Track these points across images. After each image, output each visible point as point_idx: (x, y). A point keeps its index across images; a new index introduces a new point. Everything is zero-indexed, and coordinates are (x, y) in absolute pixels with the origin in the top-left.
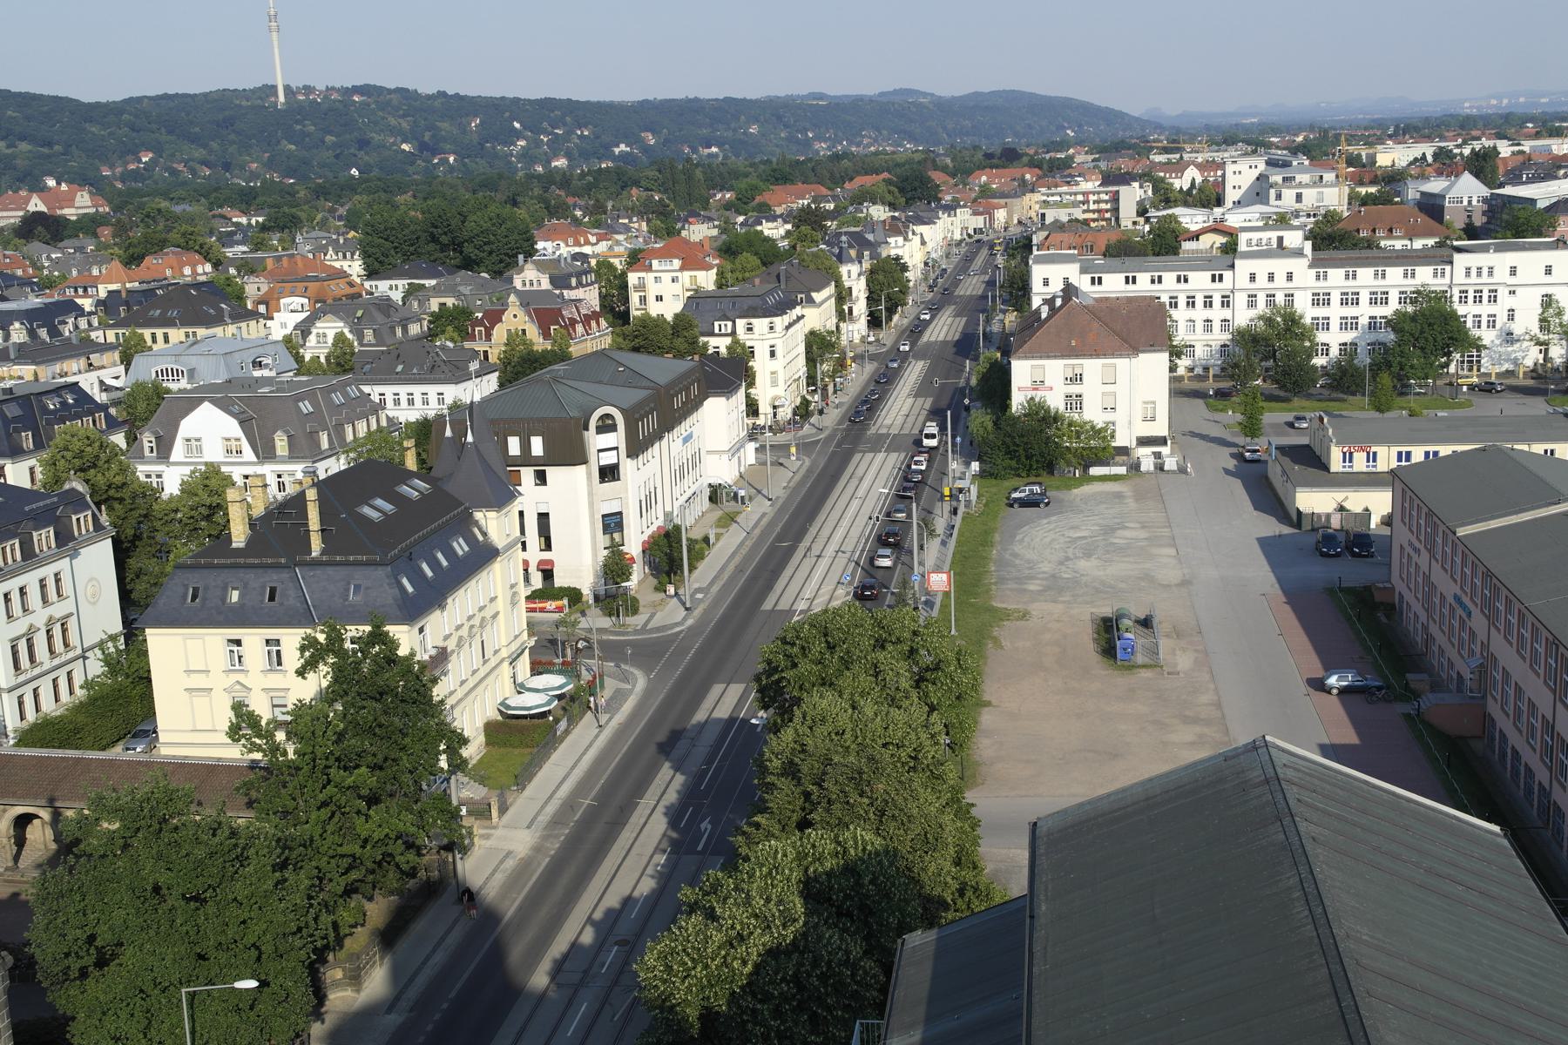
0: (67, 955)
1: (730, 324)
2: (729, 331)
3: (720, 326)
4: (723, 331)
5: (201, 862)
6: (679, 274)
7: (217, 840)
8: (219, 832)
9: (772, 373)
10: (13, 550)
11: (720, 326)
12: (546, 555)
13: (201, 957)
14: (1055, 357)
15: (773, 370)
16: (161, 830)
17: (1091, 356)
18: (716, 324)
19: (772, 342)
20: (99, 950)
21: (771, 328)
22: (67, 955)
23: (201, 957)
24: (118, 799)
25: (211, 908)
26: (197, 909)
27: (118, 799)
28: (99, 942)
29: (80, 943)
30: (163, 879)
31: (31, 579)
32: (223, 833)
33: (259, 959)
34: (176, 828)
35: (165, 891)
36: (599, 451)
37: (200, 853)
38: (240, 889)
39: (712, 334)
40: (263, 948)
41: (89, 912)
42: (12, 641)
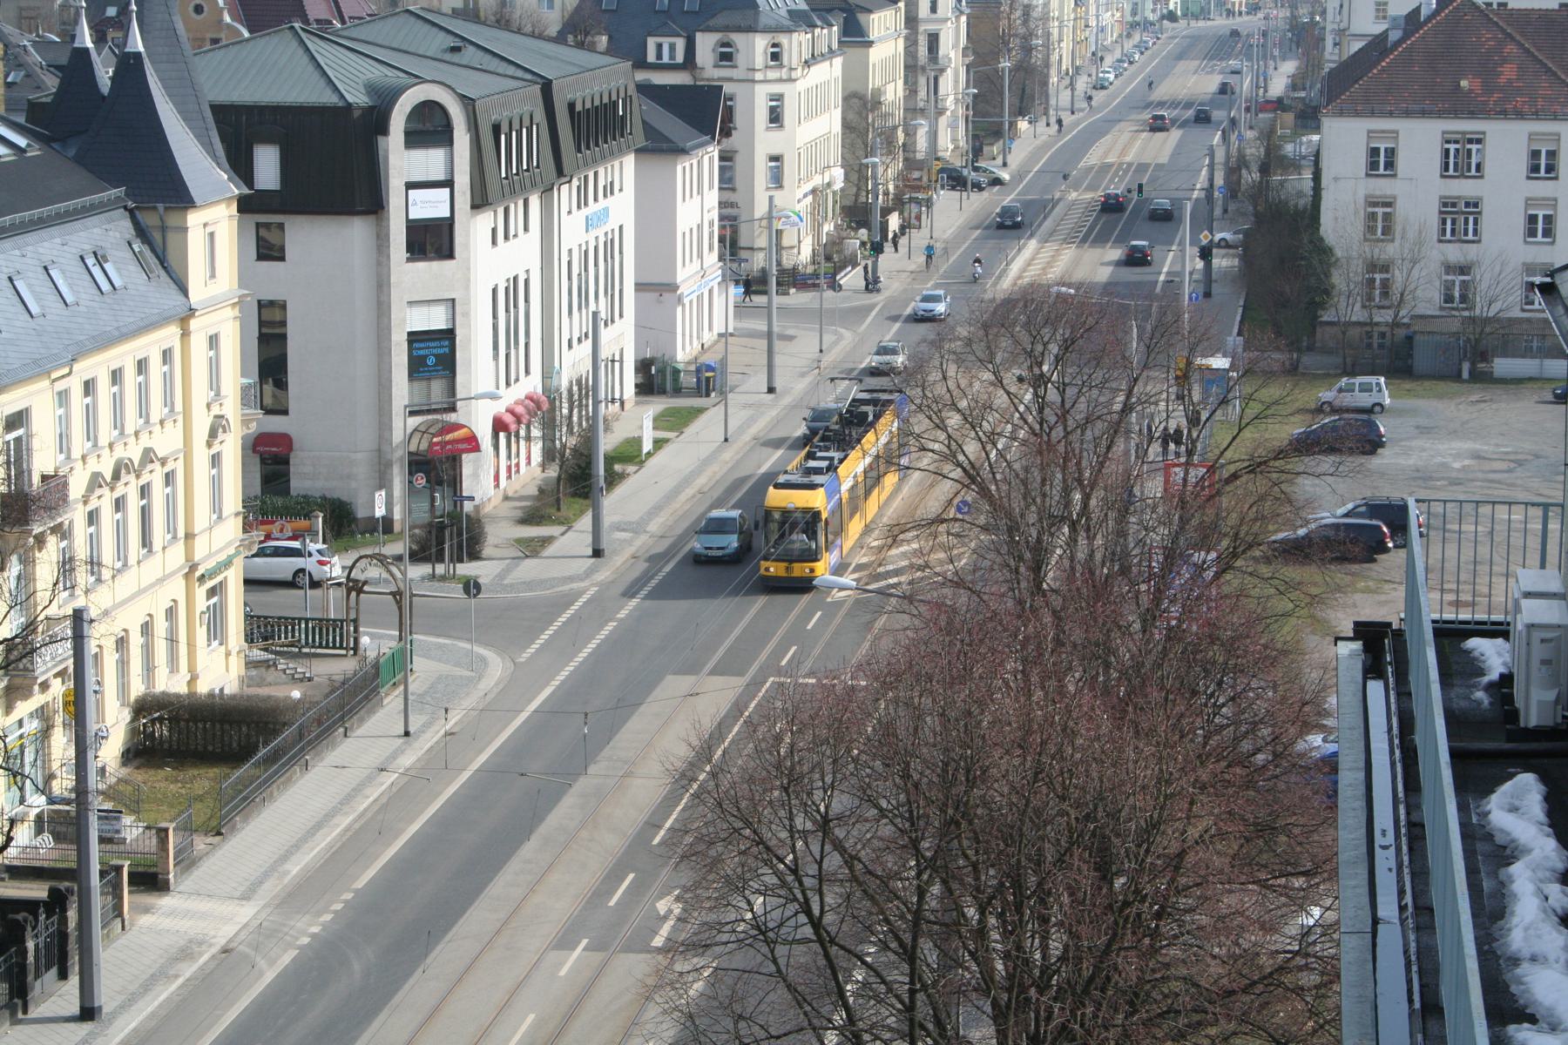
1: (680, 44)
2: (680, 58)
3: (660, 46)
4: (666, 59)
9: (775, 158)
11: (660, 46)
12: (276, 424)
14: (1424, 114)
15: (775, 152)
17: (1503, 114)
18: (651, 43)
19: (776, 89)
21: (775, 57)
36: (411, 186)
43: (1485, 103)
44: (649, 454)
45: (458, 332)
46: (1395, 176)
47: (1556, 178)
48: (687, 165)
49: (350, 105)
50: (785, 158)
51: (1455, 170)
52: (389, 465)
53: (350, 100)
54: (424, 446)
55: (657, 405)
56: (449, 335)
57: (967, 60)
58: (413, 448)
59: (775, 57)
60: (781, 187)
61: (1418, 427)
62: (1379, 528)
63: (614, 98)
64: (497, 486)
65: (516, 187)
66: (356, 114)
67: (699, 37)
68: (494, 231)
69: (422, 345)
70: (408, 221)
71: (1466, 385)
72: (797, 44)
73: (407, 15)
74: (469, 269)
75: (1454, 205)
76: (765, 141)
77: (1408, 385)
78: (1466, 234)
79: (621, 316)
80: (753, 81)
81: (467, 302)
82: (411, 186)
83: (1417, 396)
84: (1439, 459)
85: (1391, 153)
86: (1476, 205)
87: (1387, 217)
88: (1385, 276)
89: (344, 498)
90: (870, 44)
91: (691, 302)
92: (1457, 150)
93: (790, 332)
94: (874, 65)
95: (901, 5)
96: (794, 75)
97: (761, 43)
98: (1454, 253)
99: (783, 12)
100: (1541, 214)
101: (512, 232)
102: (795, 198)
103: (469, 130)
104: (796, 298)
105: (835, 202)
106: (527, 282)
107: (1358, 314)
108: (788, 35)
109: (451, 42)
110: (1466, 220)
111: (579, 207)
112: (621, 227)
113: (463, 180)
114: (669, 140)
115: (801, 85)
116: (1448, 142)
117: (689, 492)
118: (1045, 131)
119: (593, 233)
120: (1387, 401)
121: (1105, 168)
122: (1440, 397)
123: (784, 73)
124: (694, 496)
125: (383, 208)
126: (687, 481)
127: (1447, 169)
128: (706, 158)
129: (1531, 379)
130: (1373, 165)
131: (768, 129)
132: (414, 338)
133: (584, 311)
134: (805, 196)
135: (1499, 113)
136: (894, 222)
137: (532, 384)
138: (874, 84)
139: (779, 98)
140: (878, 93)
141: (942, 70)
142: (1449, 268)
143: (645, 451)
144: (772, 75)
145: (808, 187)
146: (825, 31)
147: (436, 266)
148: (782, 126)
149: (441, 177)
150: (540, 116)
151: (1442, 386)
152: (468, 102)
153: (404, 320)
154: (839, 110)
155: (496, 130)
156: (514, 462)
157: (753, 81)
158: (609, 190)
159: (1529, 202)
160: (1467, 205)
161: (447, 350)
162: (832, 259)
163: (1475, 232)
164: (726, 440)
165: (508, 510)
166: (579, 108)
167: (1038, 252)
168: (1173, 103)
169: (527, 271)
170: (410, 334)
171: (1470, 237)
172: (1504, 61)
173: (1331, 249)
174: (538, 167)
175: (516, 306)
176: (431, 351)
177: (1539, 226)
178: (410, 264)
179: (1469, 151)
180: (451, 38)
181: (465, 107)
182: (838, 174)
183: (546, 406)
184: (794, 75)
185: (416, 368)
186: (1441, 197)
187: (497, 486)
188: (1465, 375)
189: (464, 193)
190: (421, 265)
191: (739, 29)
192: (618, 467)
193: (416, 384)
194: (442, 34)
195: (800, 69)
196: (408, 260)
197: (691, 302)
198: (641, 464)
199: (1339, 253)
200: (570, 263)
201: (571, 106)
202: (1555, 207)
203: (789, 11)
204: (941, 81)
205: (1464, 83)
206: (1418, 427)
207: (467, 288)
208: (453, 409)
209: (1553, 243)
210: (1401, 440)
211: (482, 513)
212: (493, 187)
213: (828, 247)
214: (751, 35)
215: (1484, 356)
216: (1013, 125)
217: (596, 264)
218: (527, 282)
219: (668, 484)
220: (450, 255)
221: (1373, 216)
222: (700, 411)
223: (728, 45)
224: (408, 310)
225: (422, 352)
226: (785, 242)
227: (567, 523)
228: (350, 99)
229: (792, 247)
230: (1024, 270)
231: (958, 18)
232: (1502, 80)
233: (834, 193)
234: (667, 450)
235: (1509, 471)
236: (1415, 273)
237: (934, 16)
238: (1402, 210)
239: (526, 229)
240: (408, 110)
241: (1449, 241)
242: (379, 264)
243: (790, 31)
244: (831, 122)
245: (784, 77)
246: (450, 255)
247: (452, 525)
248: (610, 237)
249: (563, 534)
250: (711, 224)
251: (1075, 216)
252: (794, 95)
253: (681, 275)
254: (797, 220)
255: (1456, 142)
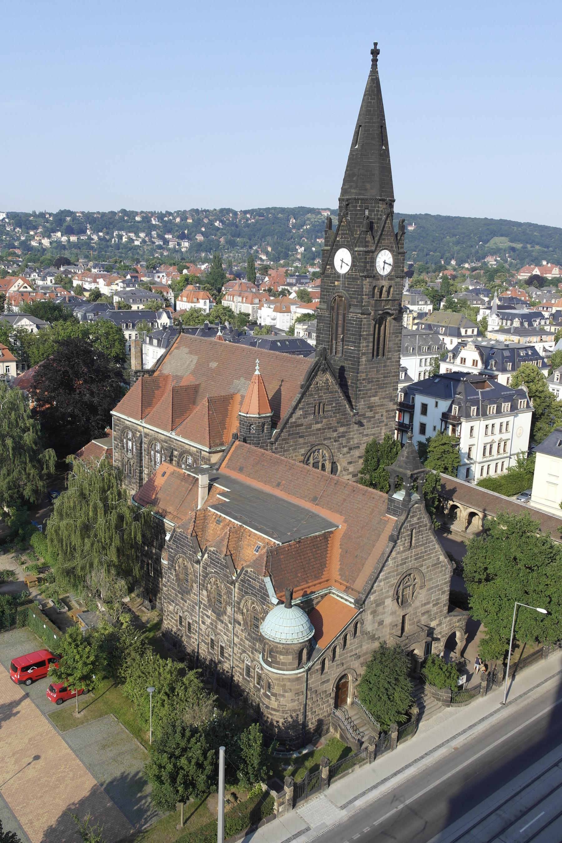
0: (475, 572)
5: (535, 554)
7: (544, 547)
8: (546, 544)
10: (493, 409)
13: (526, 593)
16: (522, 536)
20: (488, 575)
22: (475, 572)
23: (526, 593)
24: (509, 518)
25: (535, 574)
26: (529, 573)
27: (509, 518)
28: (488, 571)
29: (481, 569)
30: (519, 555)
31: (497, 422)
32: (547, 546)
33: (549, 603)
34: (528, 537)
35: (518, 561)
37: (536, 550)
38: (548, 570)
40: (553, 599)
41: (487, 558)
42: (485, 444)
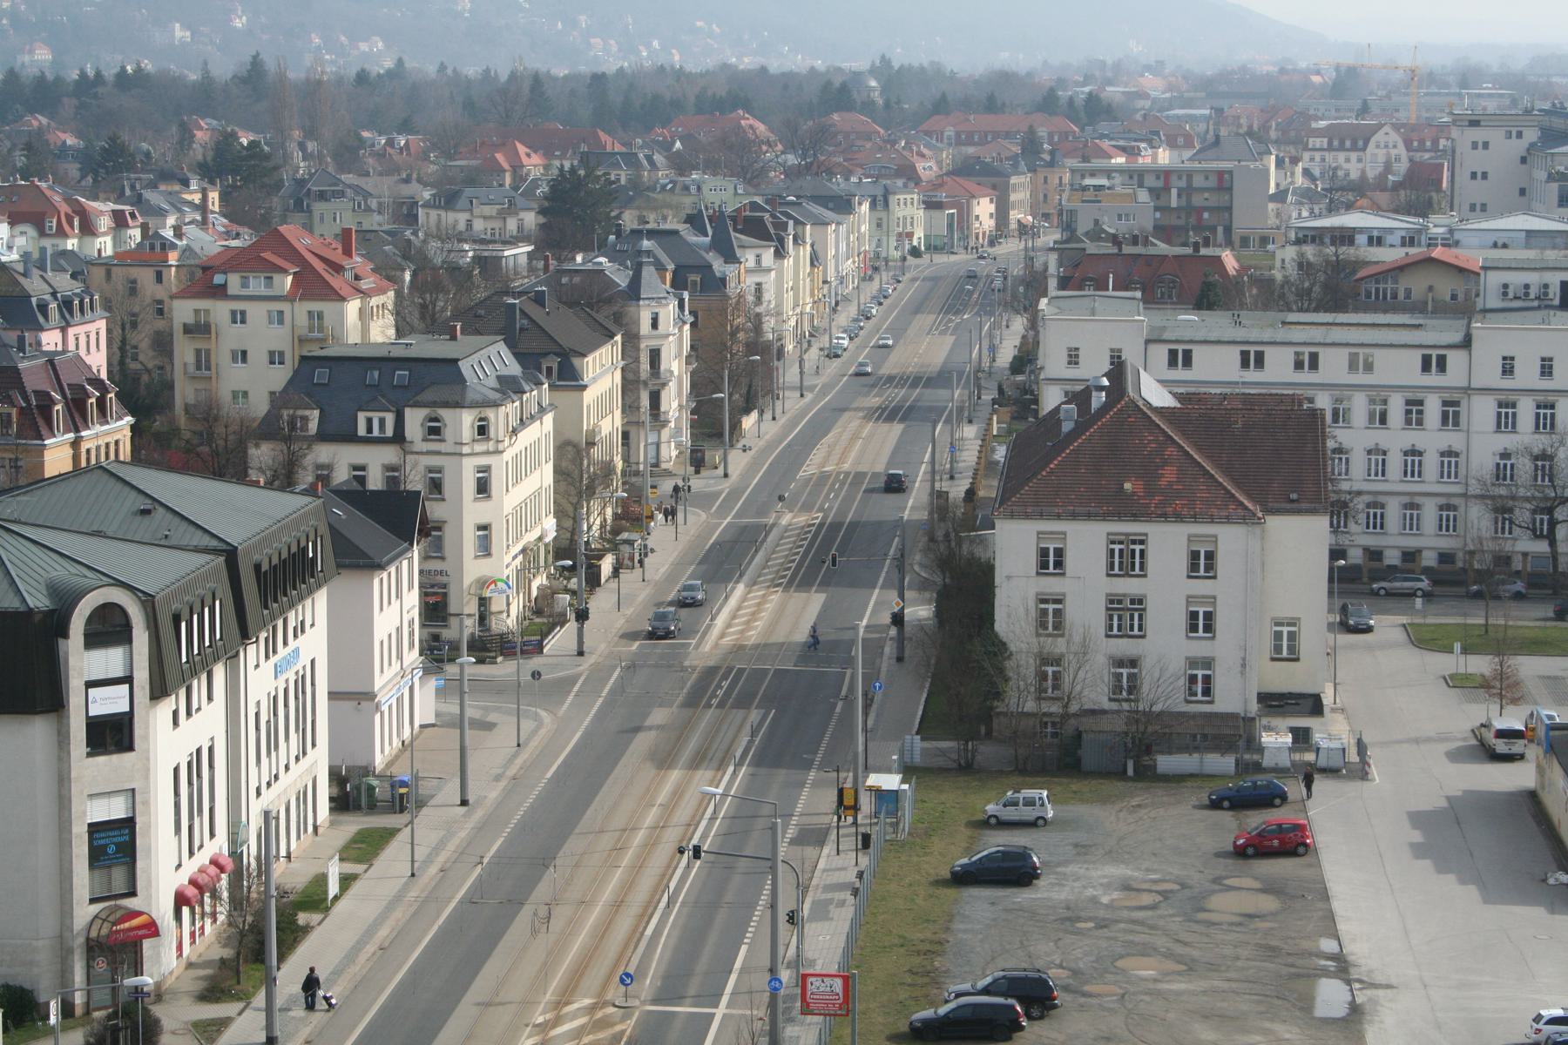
1: (390, 419)
2: (389, 432)
3: (369, 421)
6: (285, 307)
9: (484, 527)
11: (369, 421)
14: (1089, 516)
15: (483, 521)
17: (1164, 517)
18: (362, 417)
19: (483, 461)
21: (482, 430)
36: (90, 684)
39: (351, 437)
43: (1147, 506)
44: (336, 898)
45: (138, 820)
46: (1063, 574)
47: (1214, 577)
48: (385, 575)
49: (31, 609)
50: (493, 527)
51: (1120, 569)
52: (70, 951)
53: (32, 606)
54: (104, 931)
55: (353, 824)
56: (129, 823)
57: (691, 368)
58: (94, 934)
59: (482, 430)
60: (489, 555)
61: (1076, 845)
62: (1013, 1007)
63: (303, 544)
64: (180, 955)
65: (200, 666)
66: (37, 618)
67: (408, 412)
68: (175, 713)
69: (103, 835)
70: (88, 717)
71: (1130, 784)
72: (509, 411)
73: (100, 472)
74: (148, 759)
75: (1120, 602)
76: (473, 512)
77: (1075, 785)
78: (1132, 629)
79: (314, 745)
80: (461, 455)
81: (147, 791)
82: (90, 684)
83: (1083, 801)
84: (1090, 892)
85: (1059, 553)
86: (1140, 602)
87: (1058, 613)
88: (1055, 669)
89: (27, 986)
90: (584, 387)
91: (390, 707)
92: (1121, 551)
93: (492, 718)
94: (589, 407)
95: (618, 338)
96: (501, 447)
97: (467, 419)
98: (1124, 647)
99: (492, 382)
100: (1201, 610)
101: (195, 705)
102: (506, 562)
103: (148, 628)
104: (504, 669)
105: (547, 552)
106: (211, 749)
107: (1030, 706)
108: (494, 409)
109: (144, 504)
110: (1132, 618)
111: (267, 657)
112: (313, 662)
113: (142, 676)
114: (365, 555)
115: (508, 456)
116: (1113, 542)
117: (371, 948)
118: (771, 429)
119: (282, 679)
120: (1050, 814)
121: (823, 478)
122: (1104, 800)
123: (491, 446)
124: (374, 954)
125: (63, 707)
126: (370, 932)
127: (1112, 568)
128: (405, 563)
129: (1192, 776)
130: (1044, 565)
131: (476, 499)
132: (94, 828)
133: (273, 754)
134: (515, 558)
135: (1160, 516)
136: (607, 565)
137: (219, 845)
138: (588, 424)
139: (486, 469)
140: (592, 433)
141: (664, 385)
142: (1120, 663)
143: (331, 896)
144: (479, 448)
145: (519, 547)
146: (535, 393)
147: (115, 758)
148: (489, 496)
149: (119, 672)
150: (224, 589)
151: (1108, 787)
152: (148, 602)
153: (84, 813)
154: (551, 464)
155: (177, 620)
156: (198, 925)
157: (461, 455)
158: (301, 629)
159: (1190, 599)
160: (1133, 601)
161: (127, 838)
162: (543, 616)
163: (1140, 629)
164: (413, 875)
165: (193, 983)
166: (265, 567)
167: (744, 599)
168: (901, 378)
169: (212, 739)
170: (90, 825)
171: (1136, 631)
172: (1165, 463)
173: (1004, 644)
174: (221, 639)
175: (199, 776)
176: (111, 841)
177: (1201, 622)
178: (90, 759)
179: (1133, 551)
180: (141, 498)
181: (143, 602)
182: (550, 525)
183: (229, 864)
184: (501, 447)
185: (97, 857)
186: (1107, 595)
187: (180, 955)
188: (1130, 772)
189: (143, 688)
190: (101, 759)
191: (446, 405)
192: (302, 918)
193: (97, 873)
194: (134, 494)
195: (507, 439)
196: (89, 755)
197: (390, 707)
198: (327, 910)
199: (1012, 647)
200: (257, 715)
201: (257, 567)
202: (1214, 604)
203: (499, 378)
204: (664, 395)
205: (1128, 486)
206: (1076, 845)
207: (147, 777)
208: (133, 894)
209: (1213, 638)
210: (1059, 864)
211: (164, 988)
212: (171, 674)
213: (539, 601)
214: (458, 410)
215: (1148, 750)
216: (736, 426)
217: (286, 705)
218: (211, 749)
219: (348, 938)
220: (131, 748)
221: (1044, 612)
222: (390, 833)
223: (436, 420)
224: (89, 803)
225: (102, 842)
226: (494, 608)
227: (245, 997)
228: (31, 602)
229: (501, 612)
230: (729, 625)
231: (680, 330)
232: (1163, 482)
233: (546, 545)
234: (356, 888)
235: (1153, 907)
236: (1081, 674)
237: (655, 332)
238: (1072, 612)
239: (210, 698)
240: (87, 613)
241: (1116, 636)
242: (60, 759)
243: (496, 405)
244: (544, 476)
245: (491, 449)
246: (131, 748)
247: (126, 1028)
248: (301, 673)
249: (240, 1014)
250: (411, 623)
251: (787, 544)
252: (500, 468)
253: (379, 682)
254: (505, 587)
255: (1121, 543)
